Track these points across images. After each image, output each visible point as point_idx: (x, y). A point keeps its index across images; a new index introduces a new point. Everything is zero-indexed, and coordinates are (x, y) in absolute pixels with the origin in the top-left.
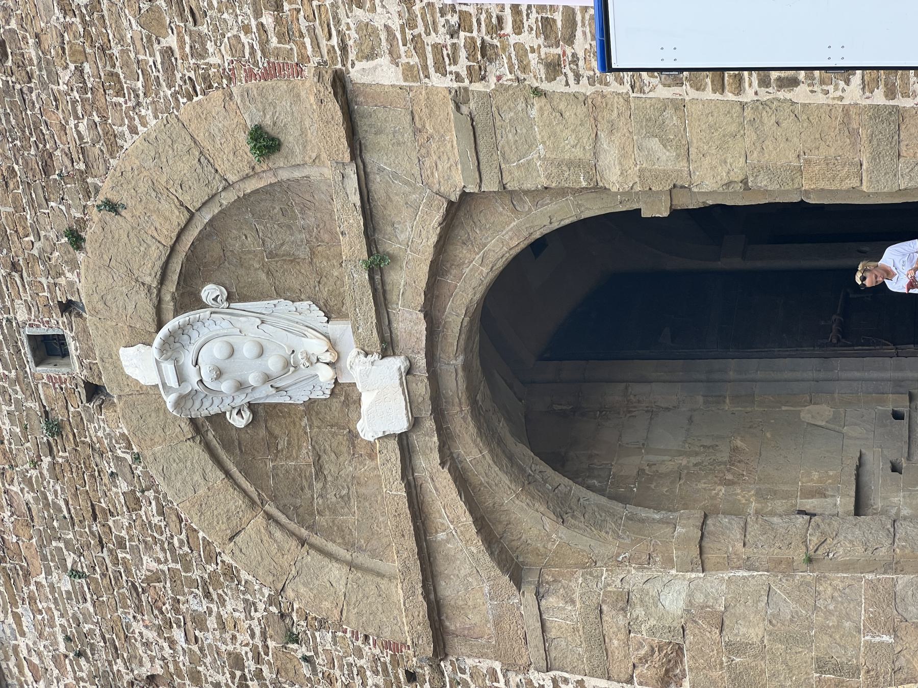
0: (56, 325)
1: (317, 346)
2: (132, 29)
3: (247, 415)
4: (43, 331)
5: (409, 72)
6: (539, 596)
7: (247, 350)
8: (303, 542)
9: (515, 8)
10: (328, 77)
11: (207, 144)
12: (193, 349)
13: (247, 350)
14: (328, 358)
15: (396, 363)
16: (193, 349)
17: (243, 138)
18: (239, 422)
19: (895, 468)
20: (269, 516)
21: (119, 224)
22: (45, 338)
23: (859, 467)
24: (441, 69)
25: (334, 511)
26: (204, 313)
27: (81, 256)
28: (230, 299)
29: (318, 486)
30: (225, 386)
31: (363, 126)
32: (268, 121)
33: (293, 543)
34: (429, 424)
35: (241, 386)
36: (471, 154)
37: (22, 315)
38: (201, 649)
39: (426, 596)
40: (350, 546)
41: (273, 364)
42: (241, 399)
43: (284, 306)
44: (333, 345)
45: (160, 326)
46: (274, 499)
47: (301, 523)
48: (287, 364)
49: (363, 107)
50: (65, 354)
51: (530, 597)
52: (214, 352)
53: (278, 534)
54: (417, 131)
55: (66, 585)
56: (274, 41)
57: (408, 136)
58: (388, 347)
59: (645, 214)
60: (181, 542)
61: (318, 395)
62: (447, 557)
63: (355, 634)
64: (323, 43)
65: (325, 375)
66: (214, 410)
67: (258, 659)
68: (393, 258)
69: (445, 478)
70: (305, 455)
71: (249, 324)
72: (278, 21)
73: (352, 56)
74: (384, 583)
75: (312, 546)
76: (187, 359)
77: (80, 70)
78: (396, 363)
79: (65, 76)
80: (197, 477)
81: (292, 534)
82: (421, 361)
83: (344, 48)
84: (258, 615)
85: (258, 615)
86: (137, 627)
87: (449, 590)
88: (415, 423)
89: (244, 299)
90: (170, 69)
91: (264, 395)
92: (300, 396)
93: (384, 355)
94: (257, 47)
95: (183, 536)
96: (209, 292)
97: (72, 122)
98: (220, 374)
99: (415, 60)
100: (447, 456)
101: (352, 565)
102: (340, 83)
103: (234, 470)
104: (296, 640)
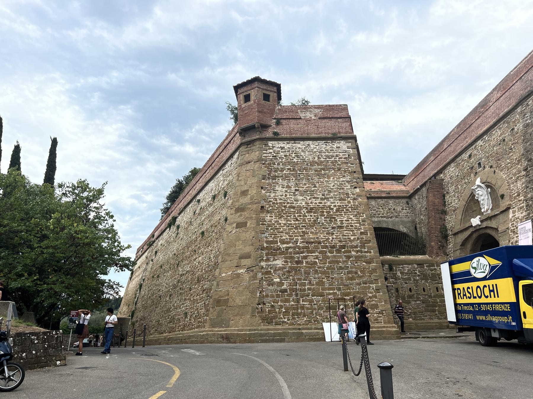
0: (482, 166)
2: (514, 171)
4: (481, 164)
5: (511, 219)
6: (460, 249)
7: (482, 198)
8: (463, 211)
9: (518, 236)
10: (509, 206)
11: (502, 187)
12: (480, 190)
13: (482, 198)
15: (479, 223)
16: (480, 190)
17: (503, 193)
20: (465, 205)
21: (493, 174)
24: (512, 225)
25: (468, 215)
27: (489, 168)
29: (471, 211)
31: (504, 213)
32: (505, 197)
33: (463, 210)
34: (475, 229)
36: (502, 231)
37: (483, 160)
39: (458, 232)
40: (464, 218)
43: (491, 202)
45: (482, 183)
46: (468, 205)
47: (466, 210)
49: (507, 213)
51: (459, 248)
52: (480, 193)
53: (464, 207)
54: (504, 222)
55: (457, 174)
56: (514, 196)
57: (504, 221)
58: (482, 221)
62: (462, 234)
63: (455, 221)
64: (514, 204)
68: (491, 220)
69: (470, 233)
70: (475, 209)
72: (516, 196)
73: (513, 209)
74: (460, 225)
75: (463, 213)
76: (479, 189)
77: (509, 163)
78: (479, 223)
79: (508, 161)
80: (468, 193)
81: (464, 209)
82: (481, 227)
83: (513, 208)
86: (454, 187)
87: (459, 235)
90: (510, 179)
93: (480, 221)
97: (503, 163)
98: (478, 194)
99: (512, 220)
101: (461, 219)
102: (508, 209)
103: (470, 198)
104: (454, 212)
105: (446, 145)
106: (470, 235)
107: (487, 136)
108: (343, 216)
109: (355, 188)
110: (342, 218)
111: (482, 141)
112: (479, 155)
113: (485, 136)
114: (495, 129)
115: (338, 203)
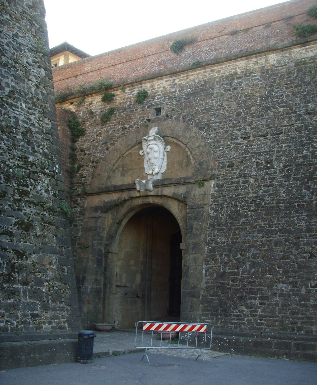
1: (156, 170)
3: (142, 154)
7: (156, 155)
14: (154, 173)
18: (141, 152)
19: (126, 294)
22: (161, 111)
23: (126, 287)
26: (164, 146)
28: (167, 152)
30: (148, 150)
34: (138, 195)
35: (148, 153)
38: (91, 142)
41: (152, 161)
42: (145, 153)
44: (157, 174)
48: (153, 164)
50: (157, 115)
52: (156, 148)
59: (181, 244)
60: (115, 138)
61: (146, 170)
65: (150, 172)
66: (143, 147)
67: (89, 154)
71: (161, 156)
77: (217, 122)
83: (219, 180)
84: (98, 155)
85: (98, 155)
88: (139, 192)
89: (167, 155)
91: (146, 158)
92: (146, 166)
94: (220, 161)
95: (117, 139)
96: (169, 148)
100: (132, 198)
105: (89, 68)
106: (125, 201)
107: (178, 79)
108: (20, 110)
109: (39, 67)
110: (18, 113)
111: (166, 81)
112: (158, 99)
113: (175, 78)
114: (194, 74)
115: (12, 81)
